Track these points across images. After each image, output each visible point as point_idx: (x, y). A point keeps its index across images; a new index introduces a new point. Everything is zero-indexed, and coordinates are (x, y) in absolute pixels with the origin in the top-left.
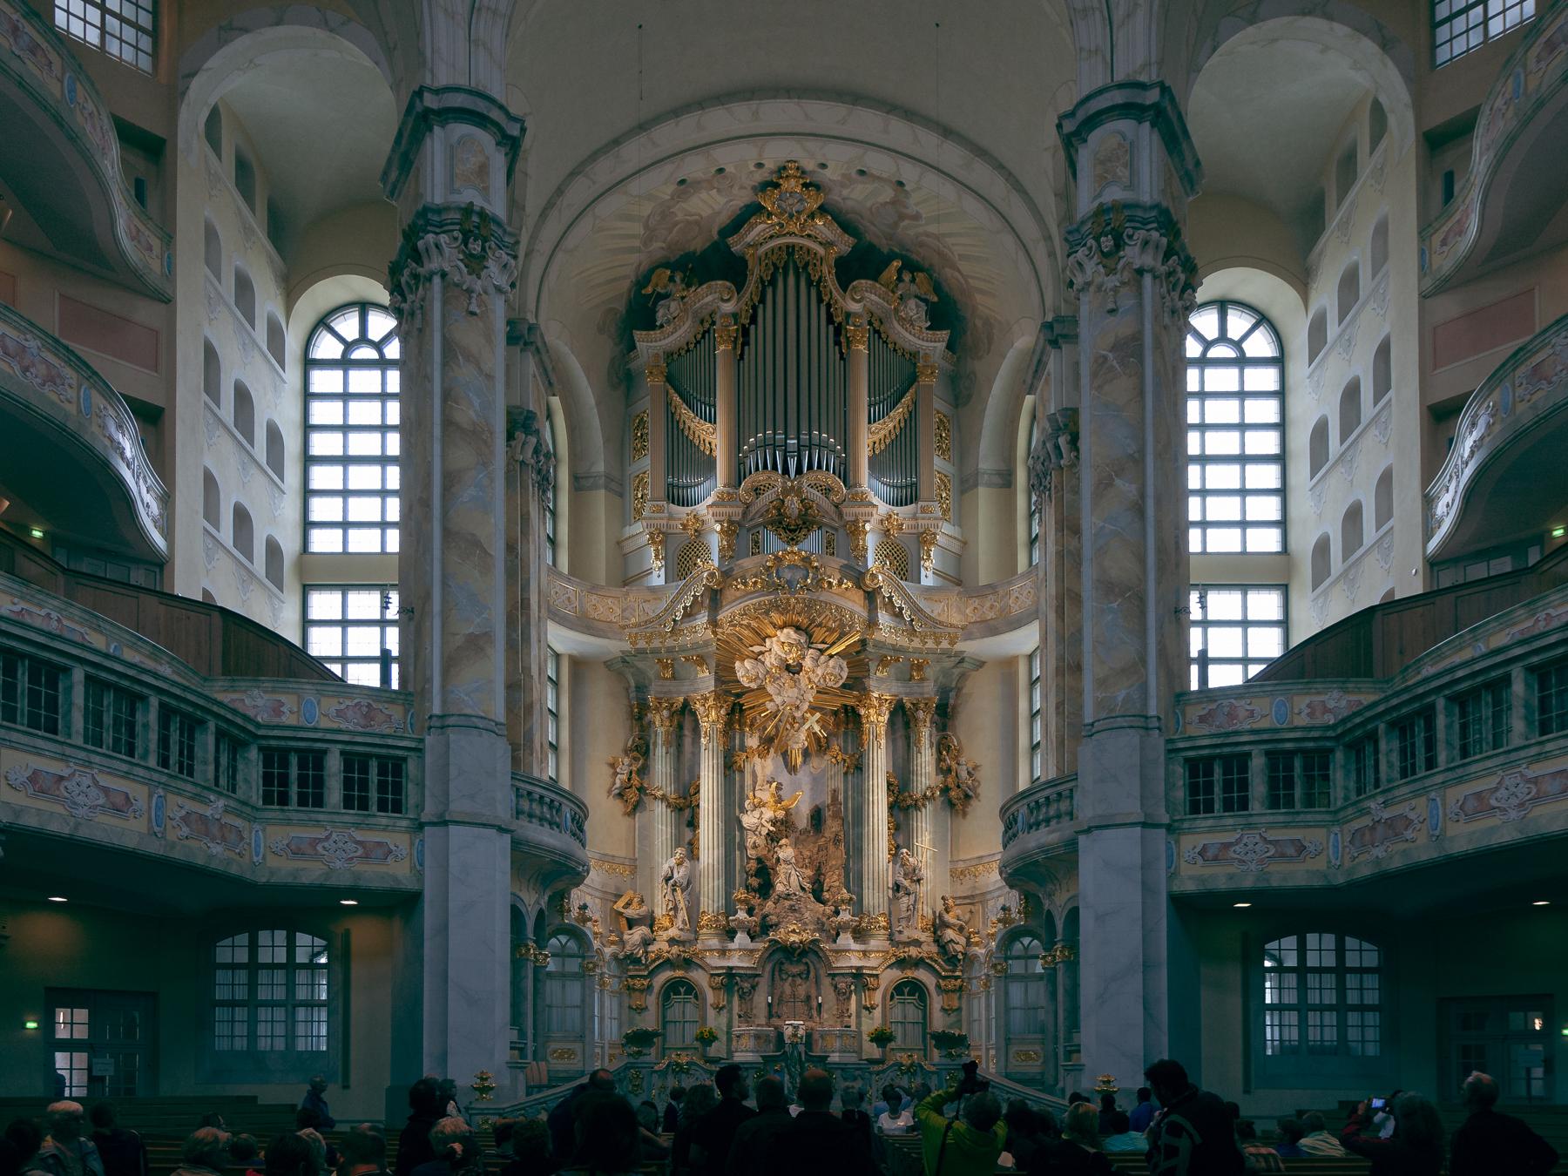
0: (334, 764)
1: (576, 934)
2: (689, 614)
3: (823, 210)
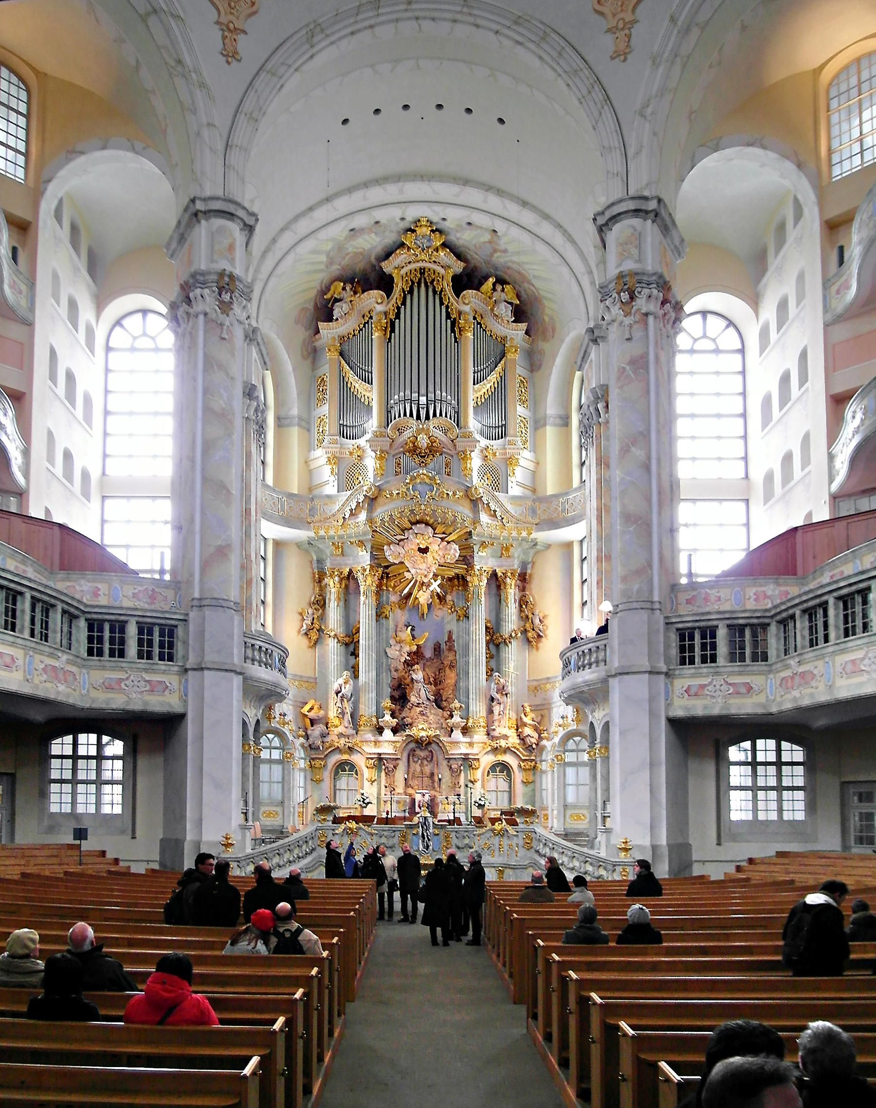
0: (132, 630)
1: (278, 733)
2: (353, 514)
3: (444, 245)
